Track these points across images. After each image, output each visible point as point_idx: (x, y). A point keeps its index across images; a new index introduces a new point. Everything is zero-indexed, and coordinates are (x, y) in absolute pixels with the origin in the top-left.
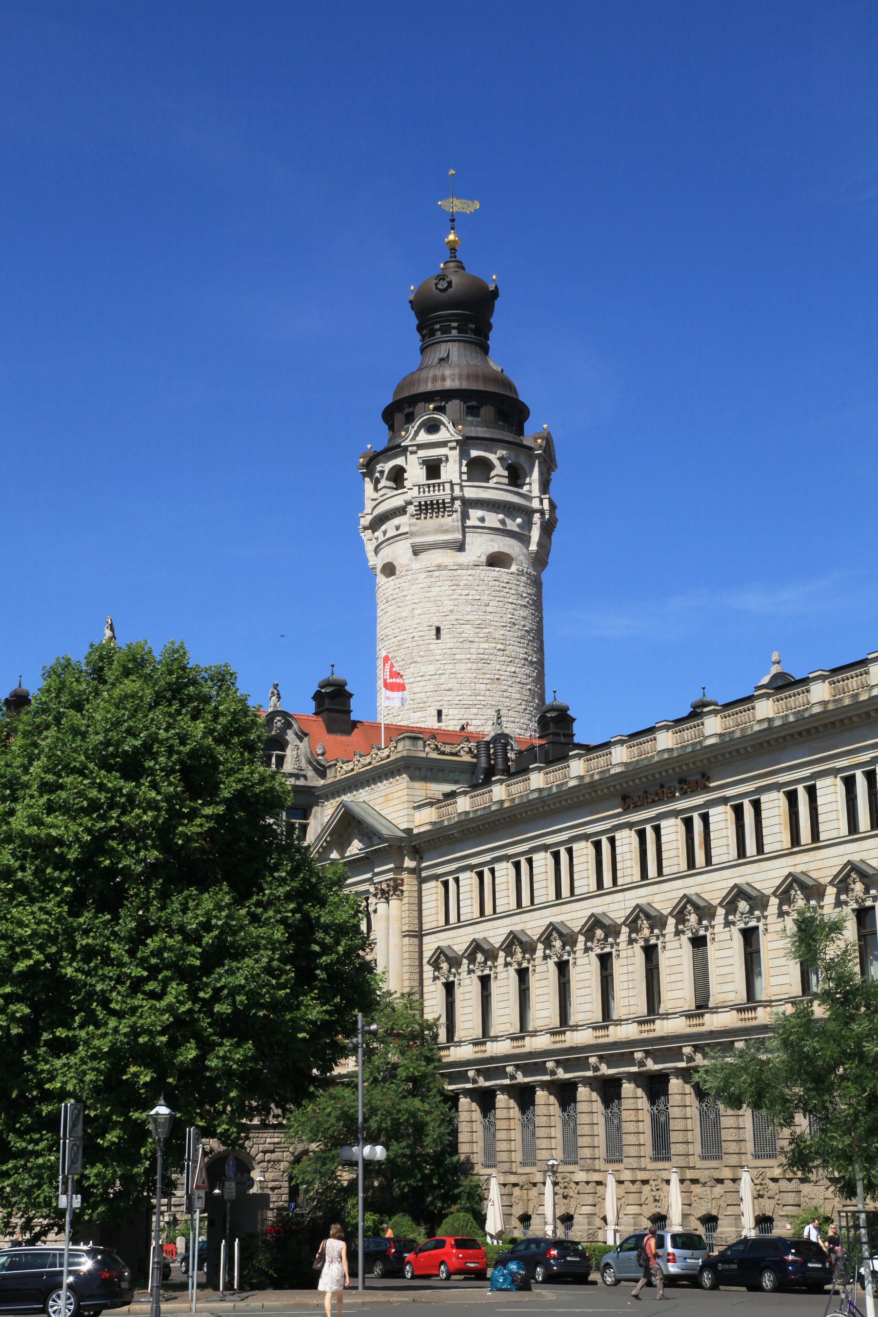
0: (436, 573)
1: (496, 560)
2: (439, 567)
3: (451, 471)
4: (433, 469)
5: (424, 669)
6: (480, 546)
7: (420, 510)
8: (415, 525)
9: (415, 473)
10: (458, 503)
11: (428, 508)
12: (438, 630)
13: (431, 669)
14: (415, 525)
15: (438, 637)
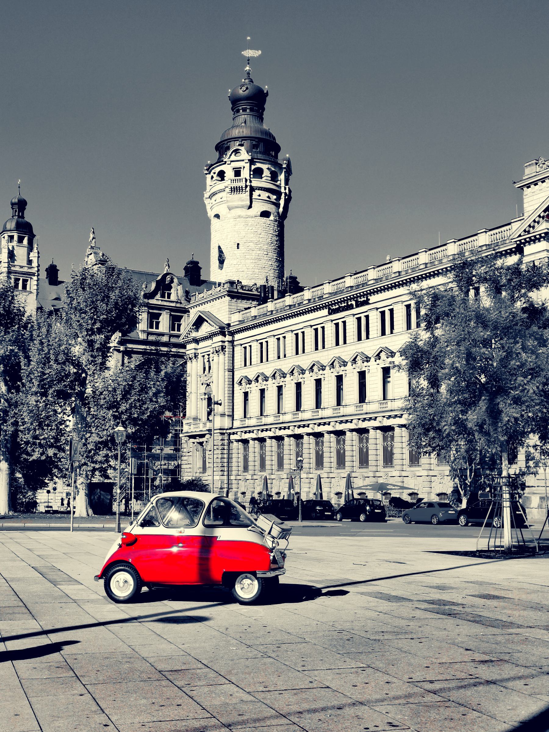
0: (238, 219)
1: (265, 214)
2: (239, 217)
3: (245, 173)
4: (237, 173)
5: (231, 262)
6: (259, 207)
7: (232, 190)
8: (229, 197)
9: (230, 174)
10: (248, 189)
11: (235, 190)
12: (238, 244)
13: (235, 262)
14: (229, 197)
15: (238, 248)
